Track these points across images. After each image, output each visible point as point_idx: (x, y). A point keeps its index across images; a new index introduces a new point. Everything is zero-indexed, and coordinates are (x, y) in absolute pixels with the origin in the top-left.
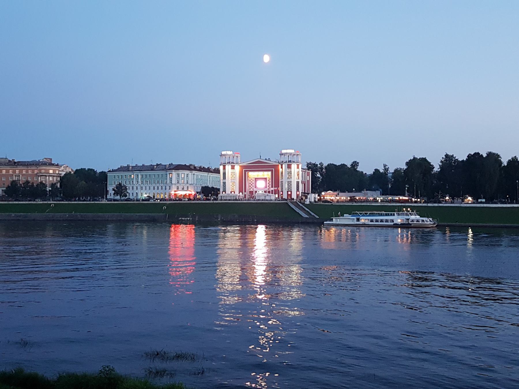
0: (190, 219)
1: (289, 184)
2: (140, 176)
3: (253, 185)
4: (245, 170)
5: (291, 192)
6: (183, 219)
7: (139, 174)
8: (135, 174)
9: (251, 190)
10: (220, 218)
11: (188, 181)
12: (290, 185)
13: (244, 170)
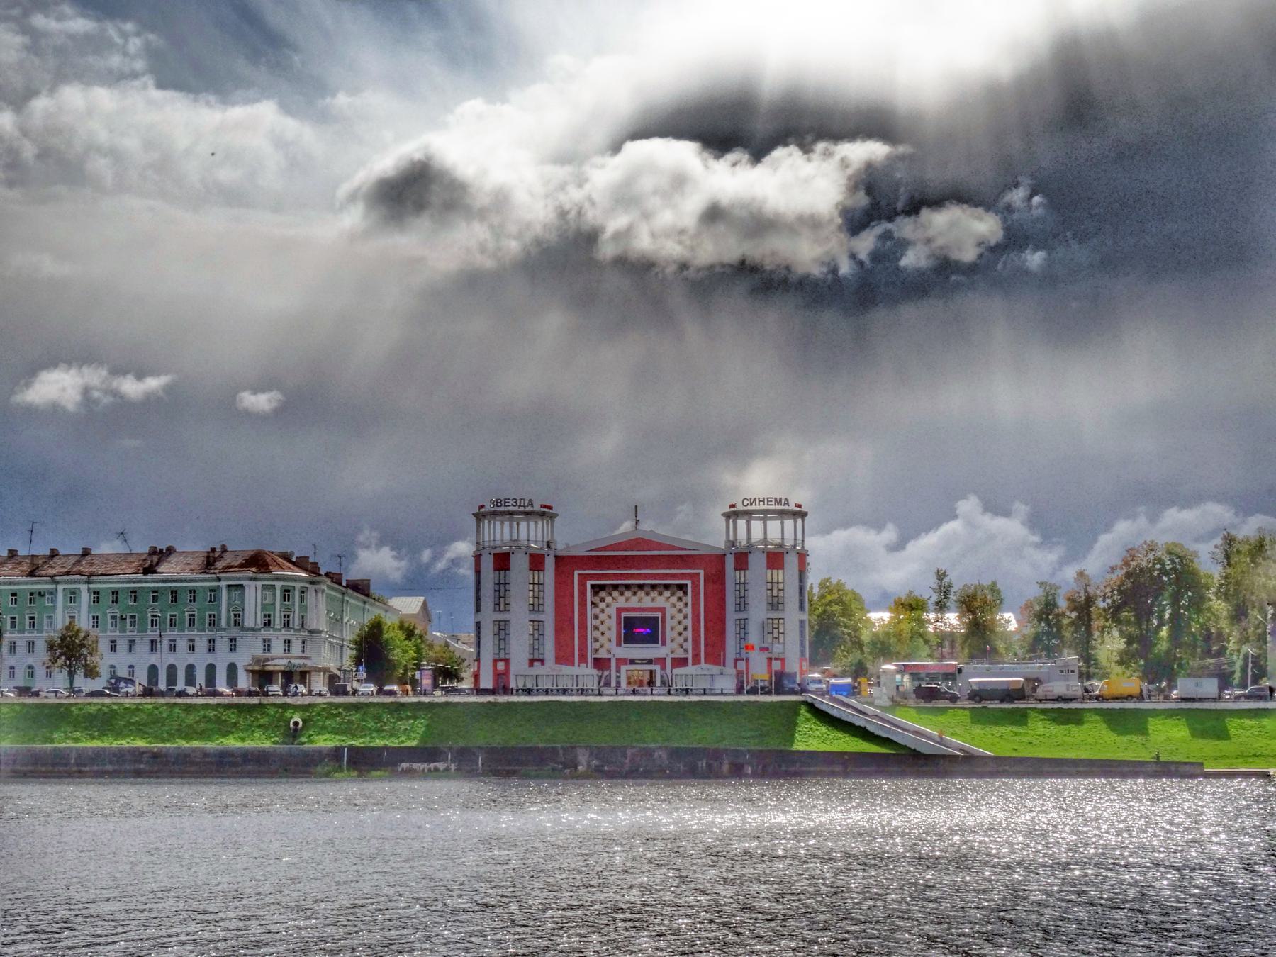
0: (447, 770)
1: (776, 635)
2: (85, 597)
4: (579, 575)
6: (415, 766)
7: (84, 587)
8: (60, 587)
9: (603, 654)
10: (585, 764)
11: (303, 617)
12: (775, 631)
13: (576, 573)
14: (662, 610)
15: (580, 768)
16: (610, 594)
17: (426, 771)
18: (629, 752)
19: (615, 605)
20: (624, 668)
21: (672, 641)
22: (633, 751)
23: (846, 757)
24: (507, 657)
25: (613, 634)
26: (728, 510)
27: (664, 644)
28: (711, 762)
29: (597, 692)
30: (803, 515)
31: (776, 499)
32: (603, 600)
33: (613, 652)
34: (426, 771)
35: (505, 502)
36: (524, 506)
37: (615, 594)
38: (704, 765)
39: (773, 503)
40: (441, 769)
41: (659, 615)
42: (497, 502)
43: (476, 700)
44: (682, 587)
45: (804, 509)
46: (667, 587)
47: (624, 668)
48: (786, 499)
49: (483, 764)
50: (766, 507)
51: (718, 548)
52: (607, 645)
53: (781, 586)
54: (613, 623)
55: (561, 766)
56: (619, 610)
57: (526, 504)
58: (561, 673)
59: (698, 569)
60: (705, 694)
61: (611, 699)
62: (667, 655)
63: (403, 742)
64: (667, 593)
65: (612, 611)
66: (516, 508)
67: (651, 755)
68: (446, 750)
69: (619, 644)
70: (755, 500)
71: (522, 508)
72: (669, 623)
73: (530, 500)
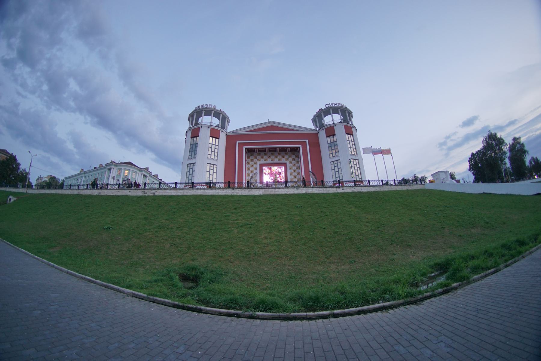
19: (259, 163)
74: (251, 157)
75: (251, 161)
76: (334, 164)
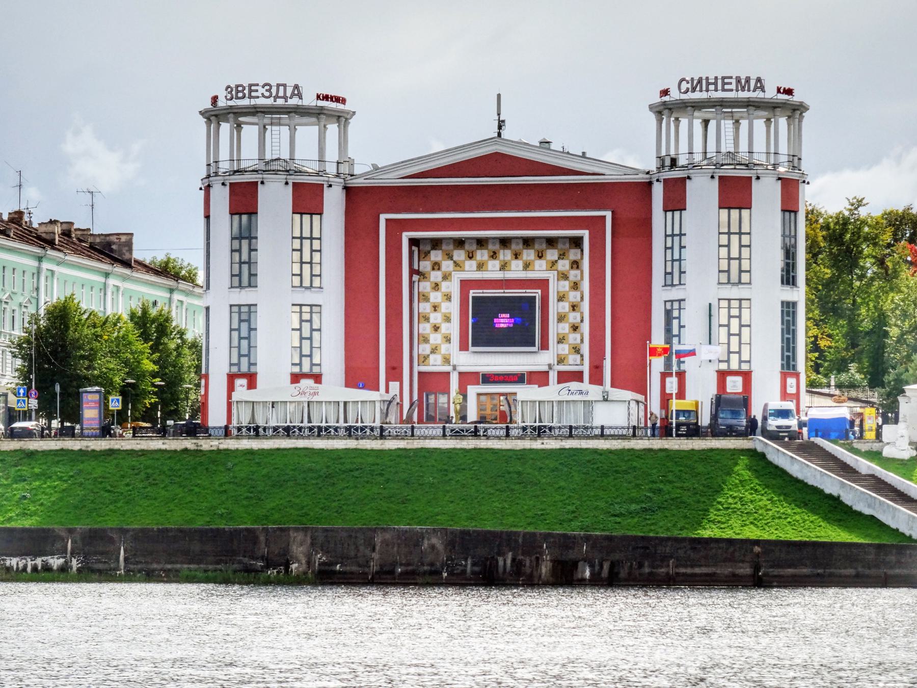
0: (64, 569)
3: (444, 328)
4: (387, 220)
5: (747, 376)
9: (435, 365)
13: (383, 217)
14: (543, 284)
15: (294, 566)
16: (450, 257)
17: (29, 569)
18: (378, 540)
19: (457, 277)
20: (473, 390)
21: (561, 340)
22: (388, 536)
23: (757, 549)
24: (253, 369)
25: (453, 329)
26: (657, 99)
27: (545, 346)
28: (521, 557)
29: (377, 432)
30: (796, 111)
31: (738, 80)
32: (436, 266)
33: (454, 361)
34: (29, 569)
35: (251, 91)
36: (285, 98)
37: (459, 255)
38: (509, 562)
39: (733, 86)
40: (55, 568)
41: (537, 293)
42: (235, 91)
43: (163, 447)
44: (577, 242)
45: (797, 98)
46: (551, 242)
47: (473, 390)
48: (759, 80)
49: (126, 559)
50: (720, 95)
51: (636, 171)
52: (444, 348)
53: (745, 240)
54: (453, 308)
55: (260, 564)
56: (466, 285)
57: (288, 94)
58: (316, 398)
59: (600, 209)
60: (571, 436)
61: (402, 444)
62: (550, 366)
63: (10, 519)
64: (552, 255)
65: (453, 287)
66: (270, 102)
67: (417, 544)
68: (63, 534)
69: (464, 347)
70: (700, 81)
71: (280, 102)
72: (554, 308)
73: (296, 87)
74: (433, 253)
75: (433, 269)
76: (729, 308)
